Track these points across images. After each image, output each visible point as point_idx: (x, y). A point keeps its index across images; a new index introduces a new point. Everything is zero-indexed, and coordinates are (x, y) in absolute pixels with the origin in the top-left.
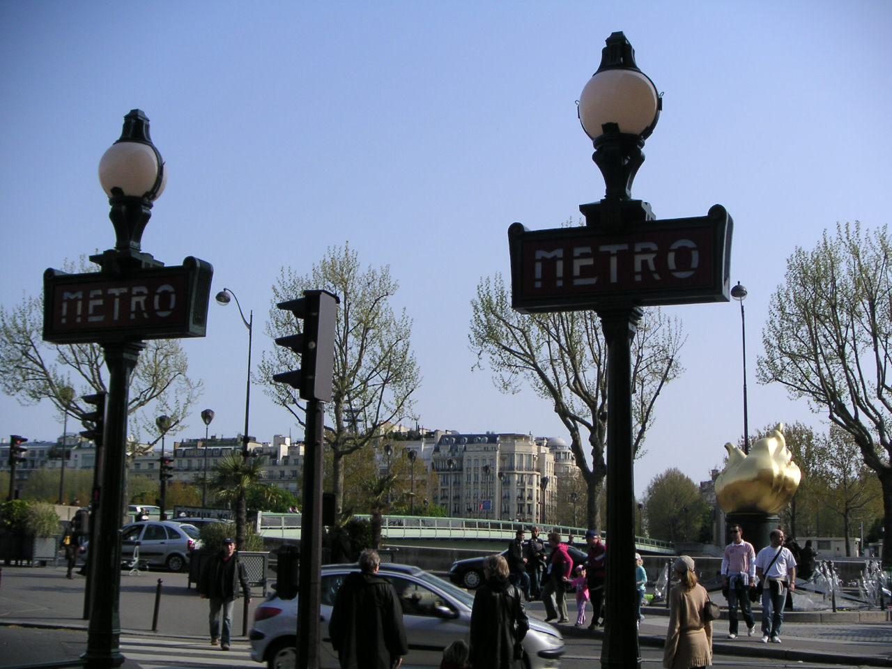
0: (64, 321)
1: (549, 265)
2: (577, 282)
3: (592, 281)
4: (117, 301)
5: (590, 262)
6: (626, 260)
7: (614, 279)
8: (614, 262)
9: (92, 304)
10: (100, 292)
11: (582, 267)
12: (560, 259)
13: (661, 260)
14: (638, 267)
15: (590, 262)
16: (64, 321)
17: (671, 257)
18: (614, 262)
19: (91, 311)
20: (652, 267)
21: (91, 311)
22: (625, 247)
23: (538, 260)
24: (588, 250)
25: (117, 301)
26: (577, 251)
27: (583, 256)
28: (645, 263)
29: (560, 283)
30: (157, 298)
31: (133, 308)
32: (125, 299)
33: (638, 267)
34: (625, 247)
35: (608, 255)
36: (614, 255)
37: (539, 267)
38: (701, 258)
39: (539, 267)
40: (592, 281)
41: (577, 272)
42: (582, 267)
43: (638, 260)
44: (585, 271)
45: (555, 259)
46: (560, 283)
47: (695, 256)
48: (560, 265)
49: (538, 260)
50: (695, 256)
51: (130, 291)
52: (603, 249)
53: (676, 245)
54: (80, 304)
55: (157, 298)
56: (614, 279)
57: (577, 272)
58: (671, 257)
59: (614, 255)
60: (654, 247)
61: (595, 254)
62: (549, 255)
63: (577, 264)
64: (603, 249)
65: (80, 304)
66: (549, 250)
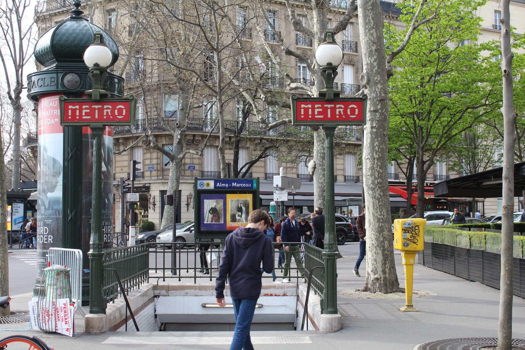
0: (78, 118)
1: (306, 110)
2: (316, 117)
3: (322, 117)
4: (97, 111)
5: (321, 110)
6: (333, 110)
7: (329, 116)
8: (329, 110)
9: (84, 111)
12: (310, 108)
13: (345, 111)
14: (337, 113)
15: (321, 110)
16: (70, 118)
17: (349, 110)
18: (329, 110)
19: (84, 114)
20: (342, 114)
21: (84, 114)
22: (333, 106)
23: (302, 108)
24: (320, 106)
25: (97, 111)
26: (84, 107)
27: (318, 108)
29: (310, 117)
30: (116, 111)
31: (105, 114)
32: (101, 111)
33: (337, 113)
34: (333, 106)
35: (327, 108)
36: (329, 108)
37: (302, 110)
39: (302, 110)
40: (322, 117)
41: (316, 113)
43: (338, 110)
44: (319, 113)
45: (76, 109)
46: (302, 117)
47: (357, 110)
48: (310, 110)
49: (302, 108)
50: (357, 110)
51: (103, 107)
52: (325, 106)
53: (350, 107)
54: (78, 111)
55: (116, 111)
56: (329, 116)
57: (316, 113)
58: (349, 110)
59: (329, 108)
60: (343, 106)
62: (306, 107)
64: (325, 106)
66: (306, 105)
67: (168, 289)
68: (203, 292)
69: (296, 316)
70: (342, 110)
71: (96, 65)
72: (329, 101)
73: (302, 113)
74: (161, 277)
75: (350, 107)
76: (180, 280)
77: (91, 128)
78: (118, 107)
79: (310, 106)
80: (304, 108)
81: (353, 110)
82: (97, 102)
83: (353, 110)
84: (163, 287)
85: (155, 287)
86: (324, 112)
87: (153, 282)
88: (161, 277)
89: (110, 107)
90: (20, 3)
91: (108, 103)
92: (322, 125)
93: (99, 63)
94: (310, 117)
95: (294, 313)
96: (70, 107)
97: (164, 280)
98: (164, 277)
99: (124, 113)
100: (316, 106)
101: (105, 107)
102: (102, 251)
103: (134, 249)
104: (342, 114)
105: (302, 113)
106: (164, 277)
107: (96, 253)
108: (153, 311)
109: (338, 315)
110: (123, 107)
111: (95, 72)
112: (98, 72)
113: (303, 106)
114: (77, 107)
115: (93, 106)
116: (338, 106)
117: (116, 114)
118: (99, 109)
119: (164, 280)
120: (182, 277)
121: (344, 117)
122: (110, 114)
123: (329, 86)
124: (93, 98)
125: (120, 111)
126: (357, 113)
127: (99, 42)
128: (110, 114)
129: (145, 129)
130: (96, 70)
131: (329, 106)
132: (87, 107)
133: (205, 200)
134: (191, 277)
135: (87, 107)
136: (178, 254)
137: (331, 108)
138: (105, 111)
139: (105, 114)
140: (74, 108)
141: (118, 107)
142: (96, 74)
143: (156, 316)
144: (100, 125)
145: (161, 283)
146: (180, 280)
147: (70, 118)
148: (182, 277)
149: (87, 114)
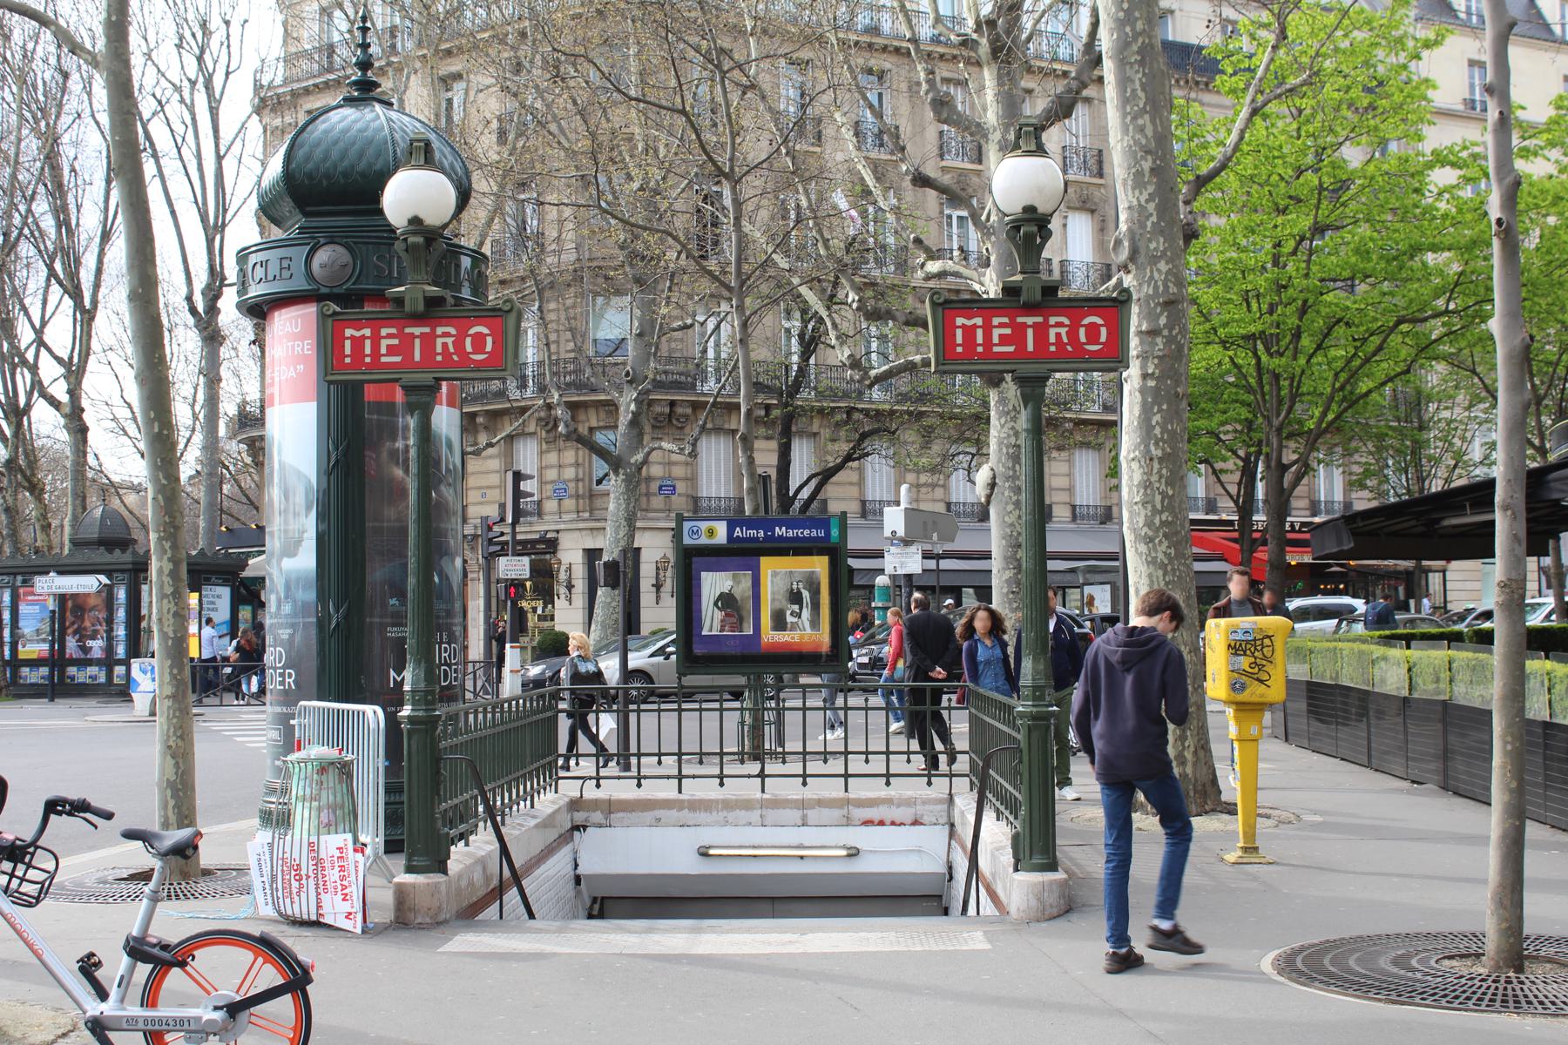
0: (368, 360)
1: (969, 332)
2: (996, 349)
3: (1011, 349)
4: (417, 342)
5: (1008, 331)
6: (1042, 331)
7: (1030, 347)
8: (1030, 332)
9: (384, 343)
10: (1005, 320)
11: (1001, 336)
14: (1052, 339)
15: (1008, 331)
16: (348, 360)
17: (1082, 331)
18: (1030, 332)
19: (383, 351)
20: (1065, 340)
21: (383, 351)
22: (1040, 319)
24: (1005, 320)
25: (417, 342)
26: (384, 332)
27: (1001, 325)
28: (1058, 335)
29: (980, 349)
31: (439, 349)
33: (1052, 339)
34: (1040, 319)
35: (1025, 326)
38: (1109, 334)
40: (1011, 349)
41: (996, 340)
42: (1000, 335)
43: (1052, 332)
44: (1004, 340)
46: (959, 349)
47: (1104, 331)
48: (980, 332)
50: (1104, 331)
51: (433, 330)
52: (1020, 320)
53: (1086, 321)
54: (368, 343)
55: (468, 341)
56: (1030, 347)
57: (996, 340)
58: (1082, 331)
60: (1067, 321)
61: (1012, 324)
62: (969, 323)
63: (996, 333)
64: (1020, 320)
65: (368, 343)
66: (969, 318)
67: (610, 807)
68: (702, 816)
69: (947, 877)
70: (1063, 331)
71: (415, 221)
72: (1030, 309)
73: (959, 340)
74: (591, 778)
75: (1086, 321)
76: (639, 785)
77: (403, 387)
78: (472, 331)
79: (979, 321)
80: (963, 326)
81: (1093, 331)
82: (417, 318)
83: (1093, 331)
84: (595, 804)
85: (575, 804)
86: (1018, 336)
87: (569, 789)
88: (591, 778)
89: (453, 331)
90: (215, 62)
91: (447, 320)
92: (1012, 372)
93: (421, 216)
94: (980, 349)
95: (943, 870)
96: (349, 332)
97: (598, 786)
98: (598, 778)
99: (489, 348)
100: (996, 321)
101: (440, 330)
102: (435, 710)
103: (518, 703)
104: (1065, 340)
105: (959, 340)
106: (598, 778)
107: (420, 713)
108: (570, 867)
109: (1060, 875)
110: (485, 330)
111: (412, 239)
112: (419, 240)
113: (960, 321)
114: (367, 332)
115: (408, 330)
116: (1053, 320)
117: (469, 348)
118: (422, 335)
119: (598, 786)
120: (645, 777)
121: (1069, 348)
122: (452, 350)
123: (1029, 267)
124: (407, 308)
125: (479, 340)
126: (1103, 338)
127: (422, 162)
128: (452, 350)
129: (542, 389)
130: (414, 233)
131: (1030, 320)
132: (393, 331)
133: (703, 574)
134: (668, 777)
135: (393, 331)
136: (633, 717)
137: (1035, 325)
138: (439, 341)
139: (439, 349)
140: (357, 334)
141: (472, 331)
142: (415, 246)
143: (578, 880)
144: (426, 378)
145: (591, 792)
146: (639, 785)
147: (348, 360)
148: (645, 777)
149: (391, 350)
